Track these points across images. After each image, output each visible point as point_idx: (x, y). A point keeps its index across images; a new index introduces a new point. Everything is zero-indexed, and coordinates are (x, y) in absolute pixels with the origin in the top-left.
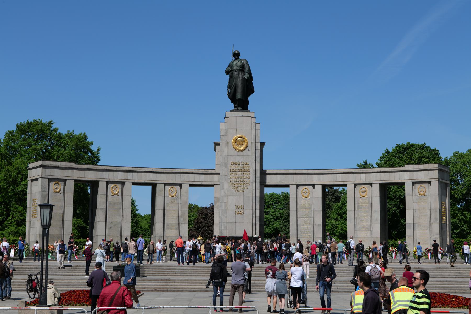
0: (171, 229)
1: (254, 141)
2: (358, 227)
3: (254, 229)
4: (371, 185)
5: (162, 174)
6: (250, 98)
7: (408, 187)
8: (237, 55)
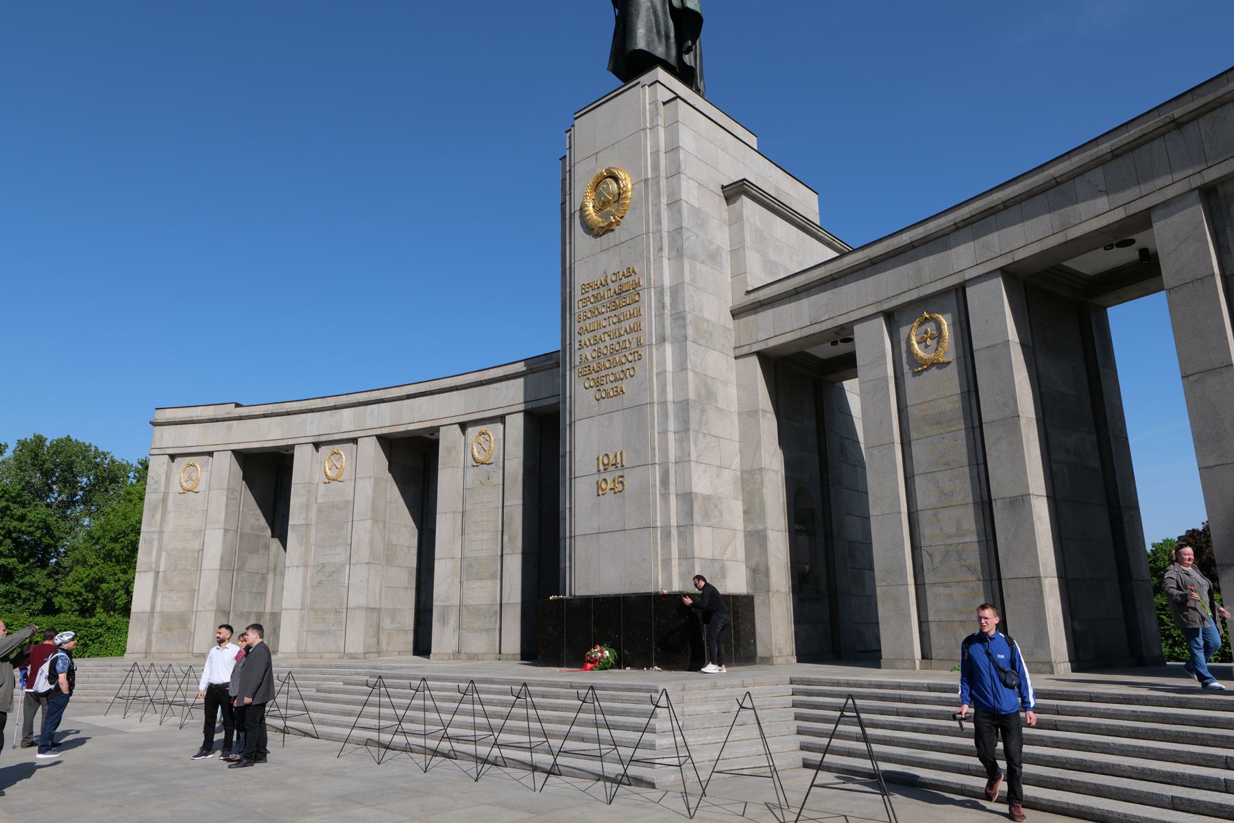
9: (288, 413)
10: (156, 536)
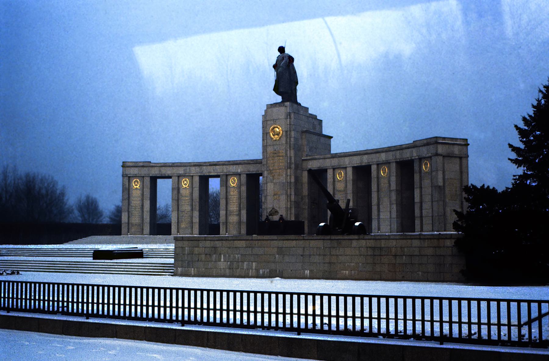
4: (389, 163)
8: (281, 49)
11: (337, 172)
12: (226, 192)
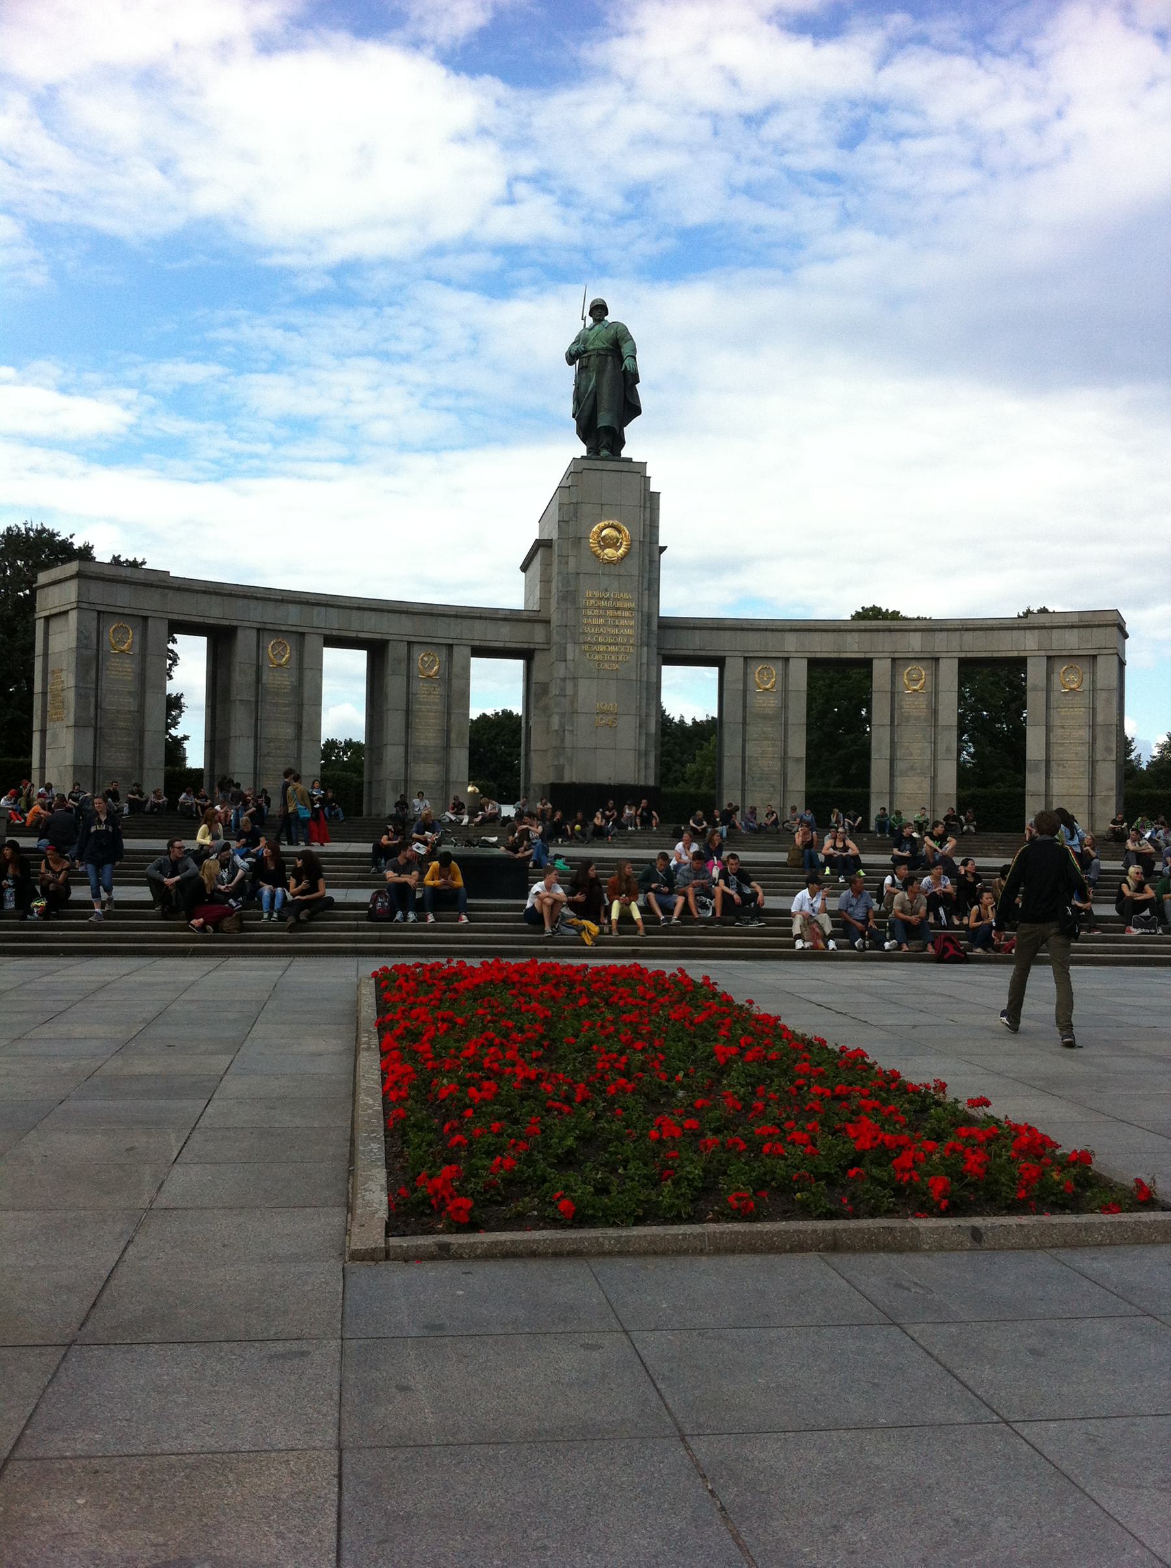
0: (425, 761)
1: (647, 539)
2: (900, 766)
3: (643, 765)
4: (937, 659)
5: (404, 616)
6: (629, 431)
7: (1035, 674)
8: (599, 310)
9: (231, 595)
10: (92, 693)
11: (757, 668)
12: (408, 693)
